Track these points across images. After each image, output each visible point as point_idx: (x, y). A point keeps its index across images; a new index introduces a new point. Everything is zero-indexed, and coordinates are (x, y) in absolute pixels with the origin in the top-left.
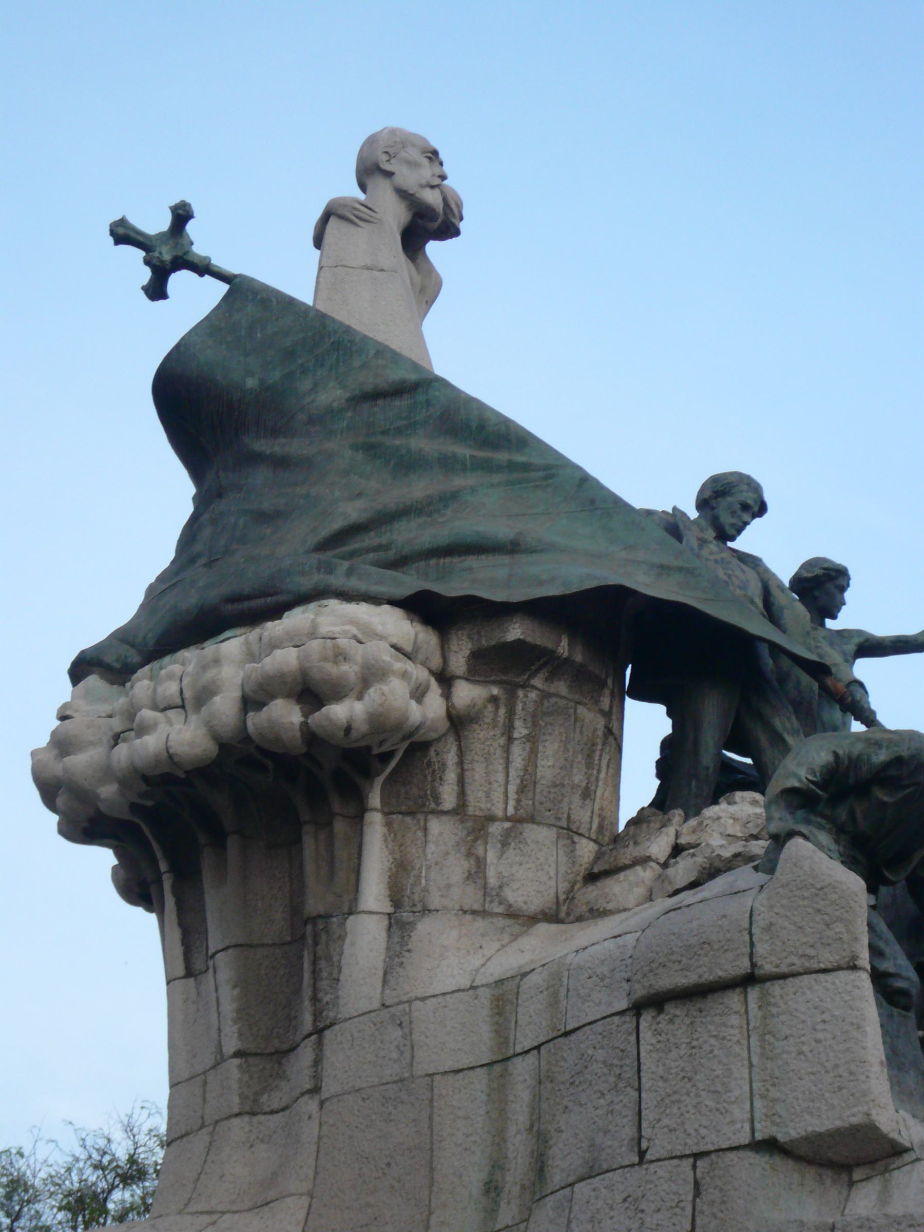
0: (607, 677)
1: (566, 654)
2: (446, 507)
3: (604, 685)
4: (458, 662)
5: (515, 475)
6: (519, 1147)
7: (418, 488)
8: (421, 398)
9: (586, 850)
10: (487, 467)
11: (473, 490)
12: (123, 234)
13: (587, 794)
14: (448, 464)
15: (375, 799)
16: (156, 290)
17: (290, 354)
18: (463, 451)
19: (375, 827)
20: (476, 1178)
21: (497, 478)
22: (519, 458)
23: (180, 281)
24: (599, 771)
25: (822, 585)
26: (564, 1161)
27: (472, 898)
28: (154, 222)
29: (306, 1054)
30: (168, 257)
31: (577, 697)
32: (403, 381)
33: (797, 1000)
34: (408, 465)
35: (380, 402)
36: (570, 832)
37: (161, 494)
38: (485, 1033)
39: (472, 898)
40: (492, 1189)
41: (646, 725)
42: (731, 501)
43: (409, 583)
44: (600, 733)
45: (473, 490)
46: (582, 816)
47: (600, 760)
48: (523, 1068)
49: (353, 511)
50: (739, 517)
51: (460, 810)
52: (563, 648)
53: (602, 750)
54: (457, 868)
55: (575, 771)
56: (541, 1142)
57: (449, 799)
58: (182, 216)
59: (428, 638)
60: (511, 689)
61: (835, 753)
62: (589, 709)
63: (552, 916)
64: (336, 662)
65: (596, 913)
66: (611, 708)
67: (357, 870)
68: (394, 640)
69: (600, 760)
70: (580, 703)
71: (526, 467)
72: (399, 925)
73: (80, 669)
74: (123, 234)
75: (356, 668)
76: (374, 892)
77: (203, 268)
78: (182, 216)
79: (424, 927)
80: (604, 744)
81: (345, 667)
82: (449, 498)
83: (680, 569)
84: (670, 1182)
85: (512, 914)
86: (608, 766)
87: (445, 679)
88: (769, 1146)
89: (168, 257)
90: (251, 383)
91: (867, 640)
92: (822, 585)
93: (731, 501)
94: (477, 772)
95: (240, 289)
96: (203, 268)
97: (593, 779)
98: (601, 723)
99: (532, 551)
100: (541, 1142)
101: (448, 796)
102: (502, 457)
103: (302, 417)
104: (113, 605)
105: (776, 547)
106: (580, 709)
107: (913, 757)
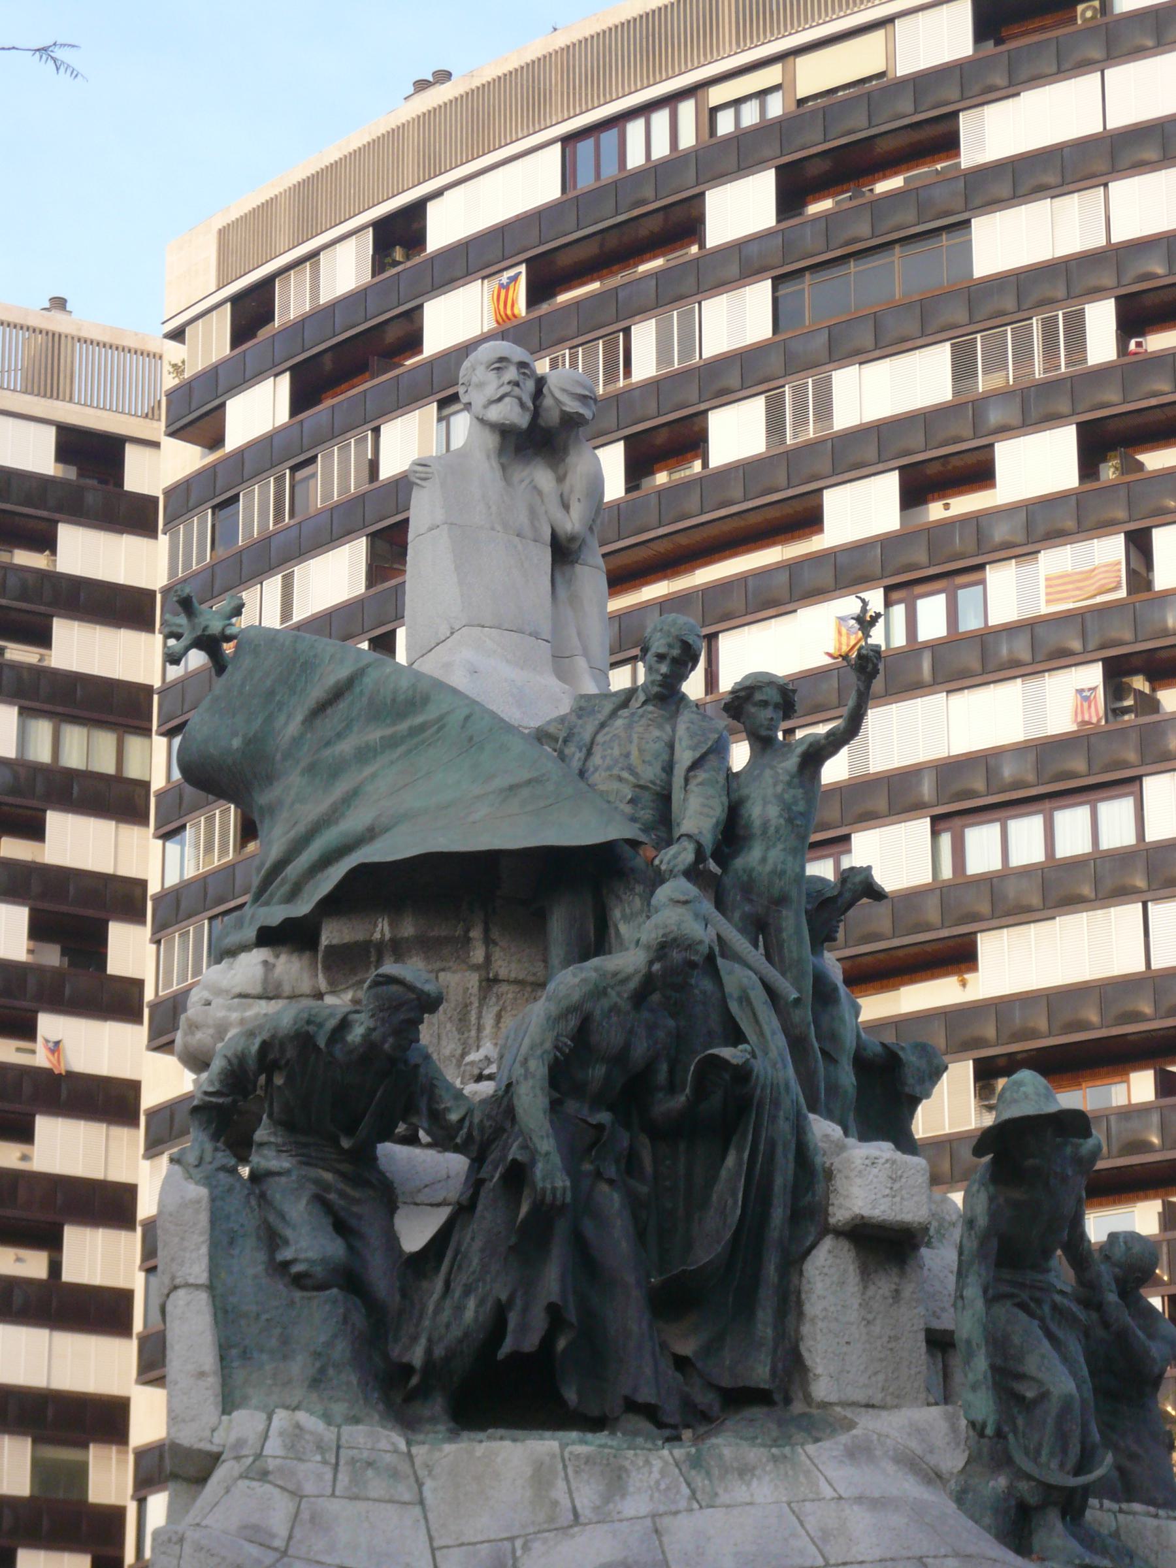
0: (467, 931)
1: (388, 936)
2: (349, 806)
3: (467, 940)
5: (416, 740)
8: (357, 690)
10: (391, 743)
11: (374, 776)
17: (271, 693)
18: (375, 734)
21: (401, 749)
22: (419, 720)
24: (480, 1029)
31: (438, 965)
32: (338, 682)
34: (336, 771)
35: (329, 711)
44: (475, 990)
45: (374, 776)
47: (479, 1017)
50: (657, 671)
52: (382, 929)
53: (481, 1007)
55: (444, 1043)
61: (225, 1056)
62: (454, 972)
64: (193, 1034)
66: (488, 958)
68: (237, 990)
69: (479, 1017)
70: (443, 970)
71: (422, 728)
75: (211, 1031)
80: (483, 999)
81: (199, 1035)
83: (529, 782)
86: (499, 1017)
90: (236, 743)
91: (811, 745)
97: (471, 1041)
98: (473, 980)
99: (386, 830)
102: (403, 726)
103: (279, 756)
106: (442, 975)
107: (273, 1037)
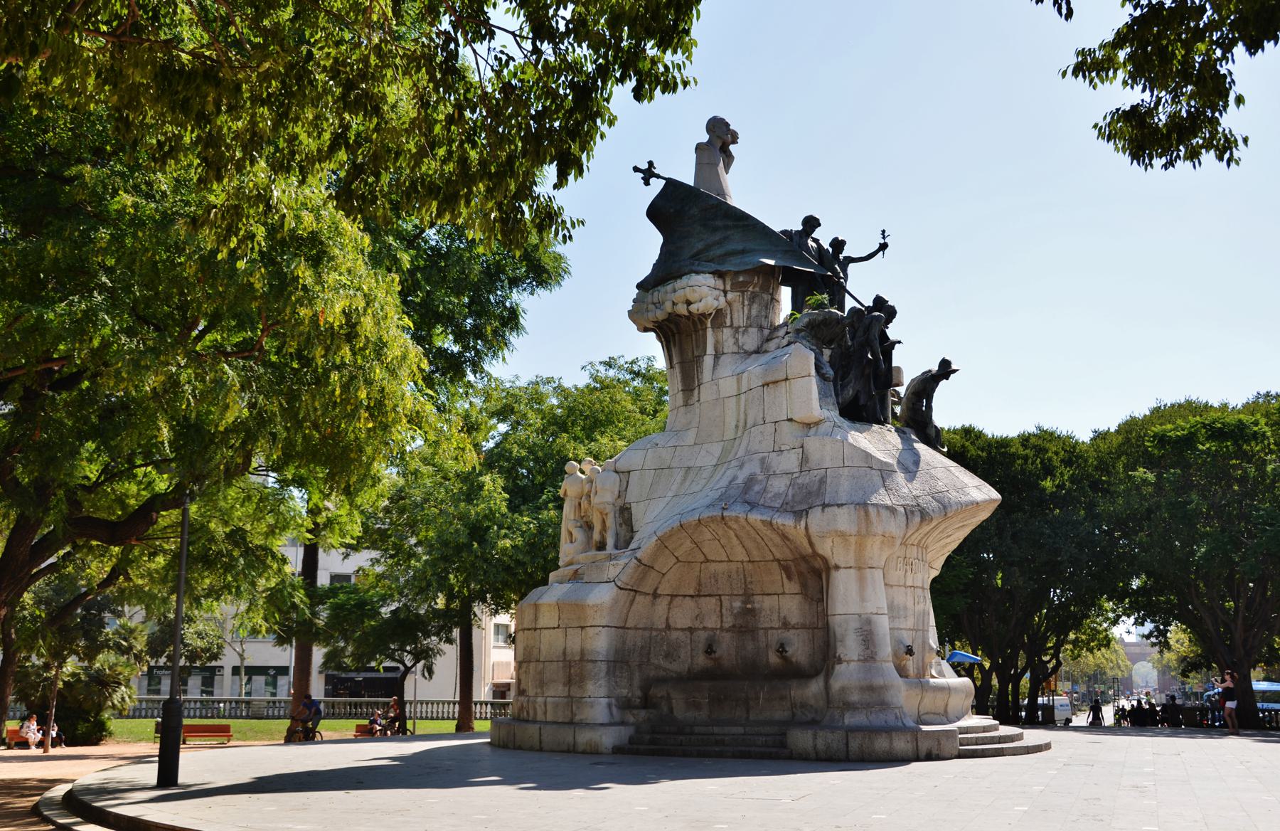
4: (728, 287)
6: (742, 416)
7: (718, 236)
9: (766, 332)
12: (636, 169)
13: (766, 317)
14: (726, 228)
15: (709, 325)
16: (647, 183)
18: (730, 223)
19: (709, 332)
20: (734, 424)
23: (653, 180)
25: (838, 244)
26: (750, 423)
27: (735, 349)
28: (645, 166)
29: (696, 392)
30: (648, 174)
33: (797, 385)
34: (715, 229)
36: (761, 328)
37: (651, 242)
38: (735, 387)
39: (735, 349)
40: (737, 426)
41: (786, 293)
42: (811, 223)
43: (714, 267)
46: (765, 324)
48: (743, 396)
49: (700, 246)
51: (731, 326)
54: (731, 341)
56: (746, 415)
57: (728, 323)
58: (651, 164)
59: (720, 283)
60: (743, 292)
63: (757, 352)
65: (766, 352)
67: (705, 343)
72: (717, 356)
73: (639, 286)
74: (636, 169)
76: (710, 349)
77: (658, 176)
78: (651, 164)
79: (723, 358)
82: (726, 238)
84: (770, 428)
85: (746, 352)
87: (725, 292)
88: (790, 420)
89: (648, 174)
92: (838, 244)
93: (811, 223)
94: (735, 316)
95: (670, 183)
96: (658, 176)
100: (746, 415)
101: (728, 323)
104: (645, 270)
105: (824, 236)
